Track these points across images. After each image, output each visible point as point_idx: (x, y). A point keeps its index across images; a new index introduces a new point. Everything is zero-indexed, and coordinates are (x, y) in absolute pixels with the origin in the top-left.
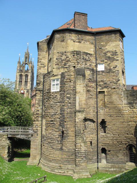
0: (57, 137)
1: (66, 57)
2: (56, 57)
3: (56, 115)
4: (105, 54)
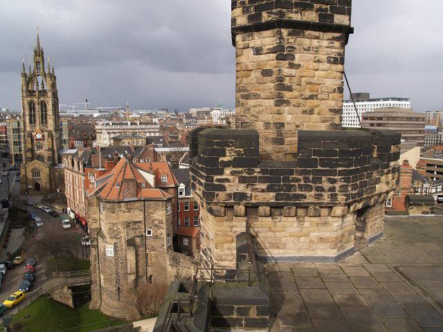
4: (153, 221)
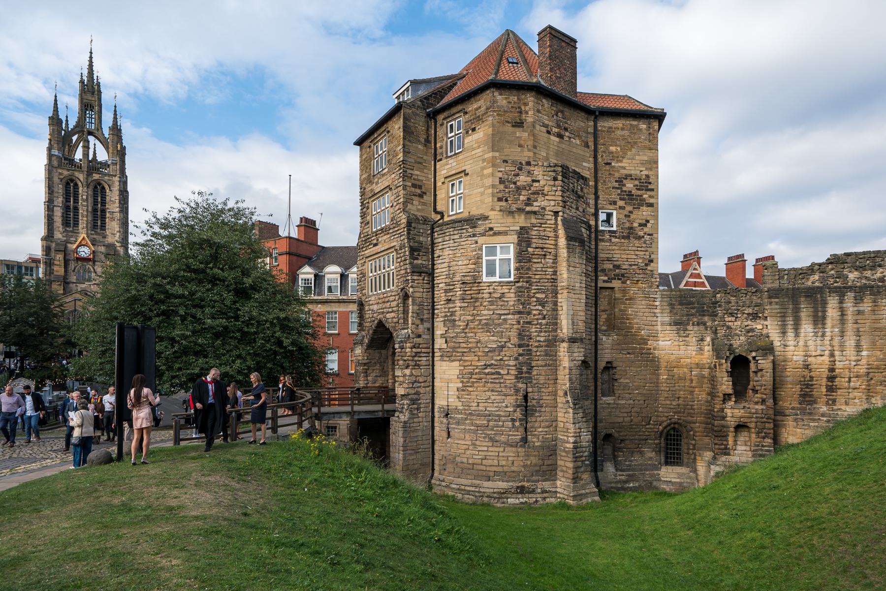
0: (509, 409)
1: (529, 179)
2: (500, 175)
3: (506, 349)
4: (620, 181)
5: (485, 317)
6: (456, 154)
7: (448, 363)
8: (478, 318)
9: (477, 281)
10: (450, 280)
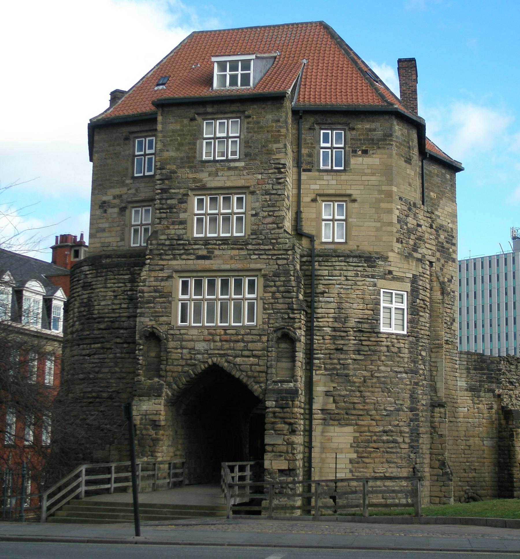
5: (382, 375)
6: (332, 170)
7: (337, 429)
8: (376, 375)
9: (376, 330)
10: (341, 325)
